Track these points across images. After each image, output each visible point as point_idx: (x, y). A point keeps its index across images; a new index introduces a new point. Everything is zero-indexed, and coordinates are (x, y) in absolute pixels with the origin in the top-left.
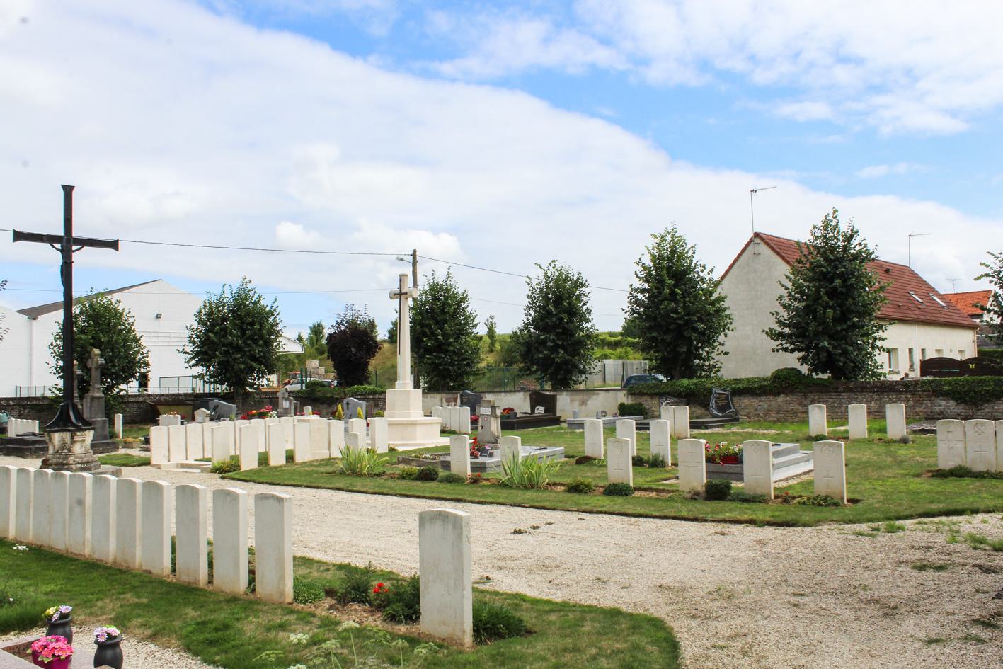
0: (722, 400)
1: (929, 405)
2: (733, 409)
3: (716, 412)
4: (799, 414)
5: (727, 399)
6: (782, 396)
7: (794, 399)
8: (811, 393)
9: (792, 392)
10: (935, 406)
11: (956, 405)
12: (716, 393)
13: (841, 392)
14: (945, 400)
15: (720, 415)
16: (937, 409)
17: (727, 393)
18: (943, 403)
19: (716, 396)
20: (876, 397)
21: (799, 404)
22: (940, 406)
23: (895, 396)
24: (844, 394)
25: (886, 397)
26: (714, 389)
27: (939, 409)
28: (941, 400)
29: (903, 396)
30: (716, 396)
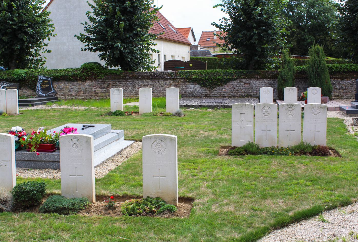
0: (46, 84)
1: (184, 88)
2: (53, 91)
4: (99, 94)
5: (49, 83)
6: (88, 81)
7: (97, 84)
8: (108, 79)
9: (95, 79)
10: (188, 88)
11: (200, 88)
12: (40, 79)
13: (128, 79)
14: (193, 85)
15: (44, 95)
16: (189, 90)
17: (49, 79)
18: (193, 86)
19: (41, 81)
20: (150, 82)
21: (99, 87)
22: (191, 88)
23: (163, 82)
24: (130, 80)
25: (157, 82)
26: (40, 77)
27: (190, 90)
28: (191, 84)
29: (168, 82)
30: (41, 81)
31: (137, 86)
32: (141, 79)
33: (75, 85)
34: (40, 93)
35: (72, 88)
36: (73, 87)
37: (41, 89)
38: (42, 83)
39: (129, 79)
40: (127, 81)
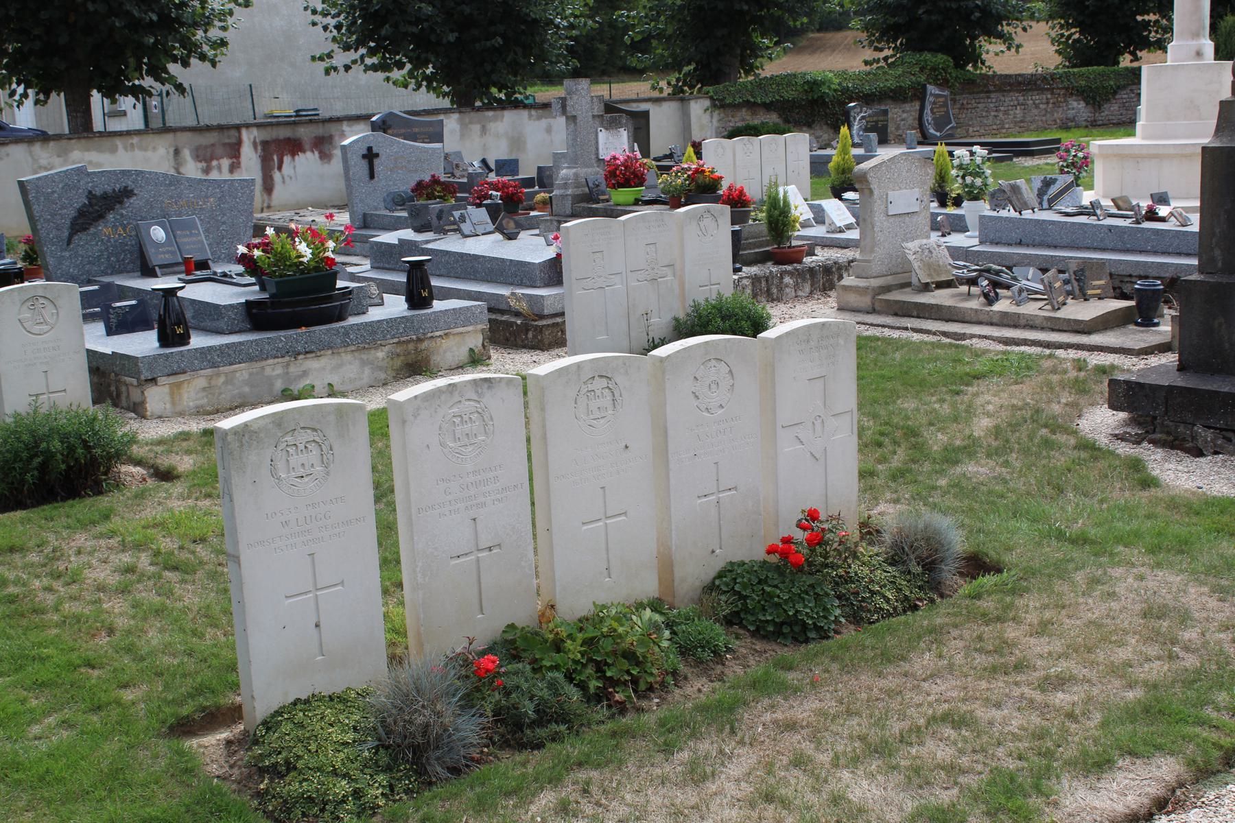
2: (953, 124)
3: (932, 131)
5: (945, 105)
12: (931, 94)
15: (938, 134)
19: (932, 99)
30: (932, 99)
31: (1002, 108)
32: (1010, 91)
33: (907, 112)
34: (932, 131)
35: (903, 120)
36: (905, 115)
37: (933, 119)
38: (934, 103)
39: (994, 92)
40: (988, 97)
